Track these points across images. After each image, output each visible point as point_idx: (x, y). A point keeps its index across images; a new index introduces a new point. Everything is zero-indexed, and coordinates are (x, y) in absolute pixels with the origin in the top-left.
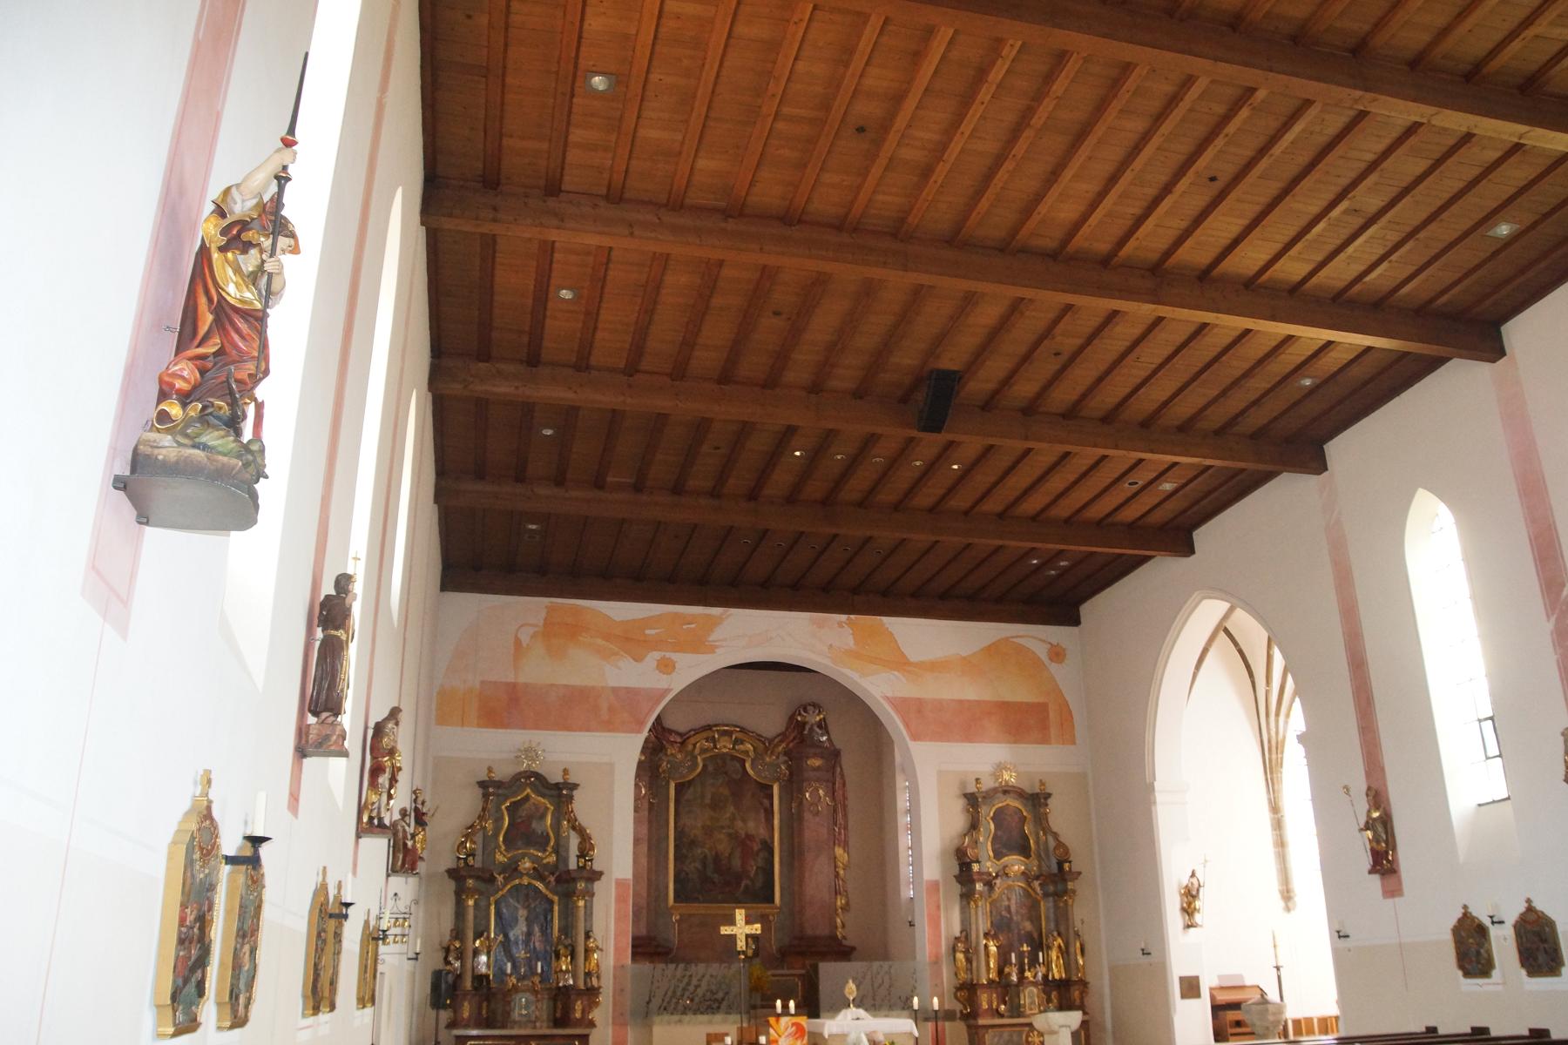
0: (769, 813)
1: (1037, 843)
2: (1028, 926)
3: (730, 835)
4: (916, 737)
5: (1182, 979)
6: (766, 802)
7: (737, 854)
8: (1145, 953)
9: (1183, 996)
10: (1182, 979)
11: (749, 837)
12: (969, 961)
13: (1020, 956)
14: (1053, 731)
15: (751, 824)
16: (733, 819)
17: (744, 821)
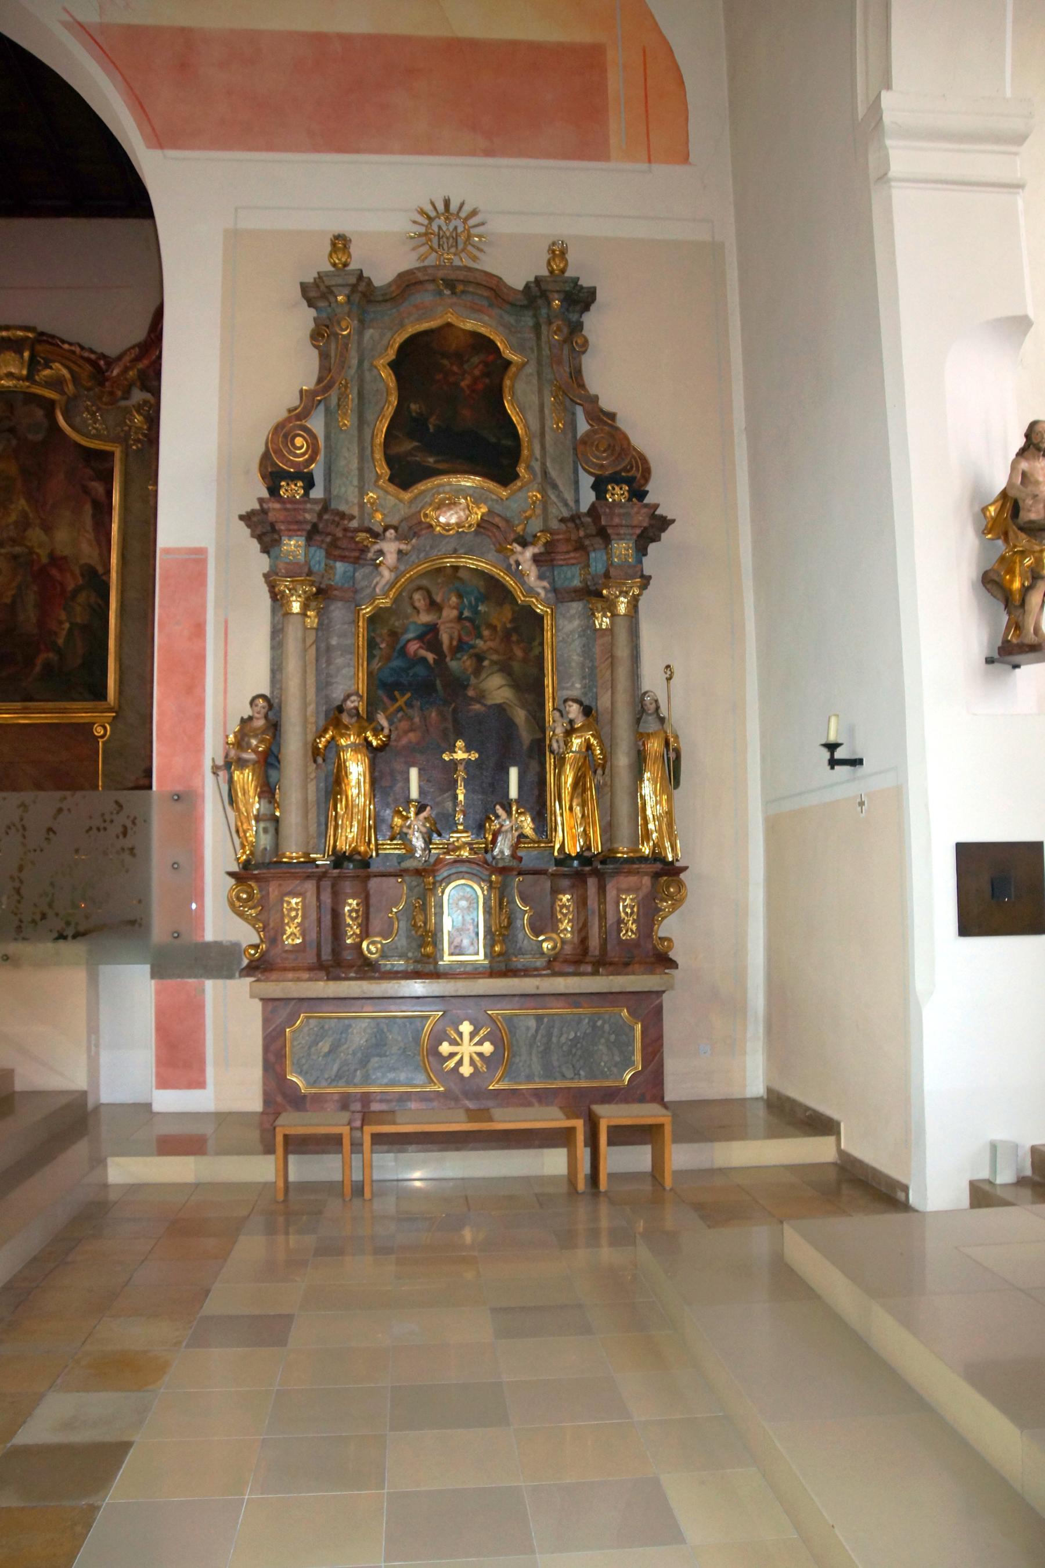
0: (102, 510)
1: (526, 426)
2: (497, 689)
3: (15, 557)
4: (159, 140)
5: (968, 856)
6: (98, 487)
7: (31, 598)
8: (836, 757)
9: (971, 923)
10: (968, 856)
11: (57, 561)
12: (268, 790)
13: (442, 778)
14: (617, 126)
15: (62, 537)
16: (24, 524)
17: (47, 529)
